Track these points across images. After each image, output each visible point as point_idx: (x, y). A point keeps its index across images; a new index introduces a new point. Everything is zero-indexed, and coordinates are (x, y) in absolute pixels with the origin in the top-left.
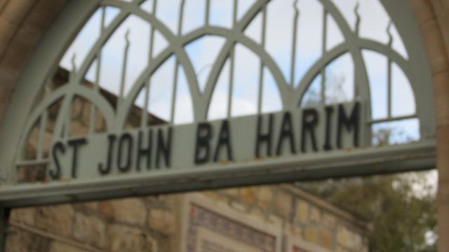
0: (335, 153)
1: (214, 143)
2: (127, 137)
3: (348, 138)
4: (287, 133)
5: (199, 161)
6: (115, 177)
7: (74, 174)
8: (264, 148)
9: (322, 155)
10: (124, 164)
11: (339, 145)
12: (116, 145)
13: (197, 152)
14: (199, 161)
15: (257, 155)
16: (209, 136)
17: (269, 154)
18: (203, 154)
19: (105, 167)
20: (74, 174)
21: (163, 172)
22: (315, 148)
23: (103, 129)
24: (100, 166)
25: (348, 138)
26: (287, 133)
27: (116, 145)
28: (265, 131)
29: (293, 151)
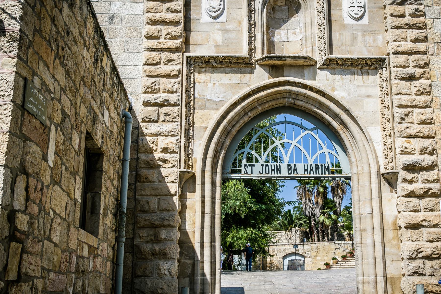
0: (324, 175)
1: (292, 170)
2: (267, 165)
3: (327, 173)
4: (311, 170)
5: (289, 174)
6: (264, 175)
7: (252, 174)
8: (306, 172)
9: (320, 175)
10: (267, 172)
11: (325, 174)
12: (264, 167)
13: (288, 172)
14: (289, 174)
15: (304, 174)
16: (291, 168)
17: (307, 174)
18: (290, 172)
19: (261, 172)
20: (252, 174)
21: (279, 175)
22: (319, 174)
23: (257, 161)
24: (260, 172)
25: (327, 173)
26: (311, 170)
27: (264, 167)
28: (306, 168)
29: (314, 174)
